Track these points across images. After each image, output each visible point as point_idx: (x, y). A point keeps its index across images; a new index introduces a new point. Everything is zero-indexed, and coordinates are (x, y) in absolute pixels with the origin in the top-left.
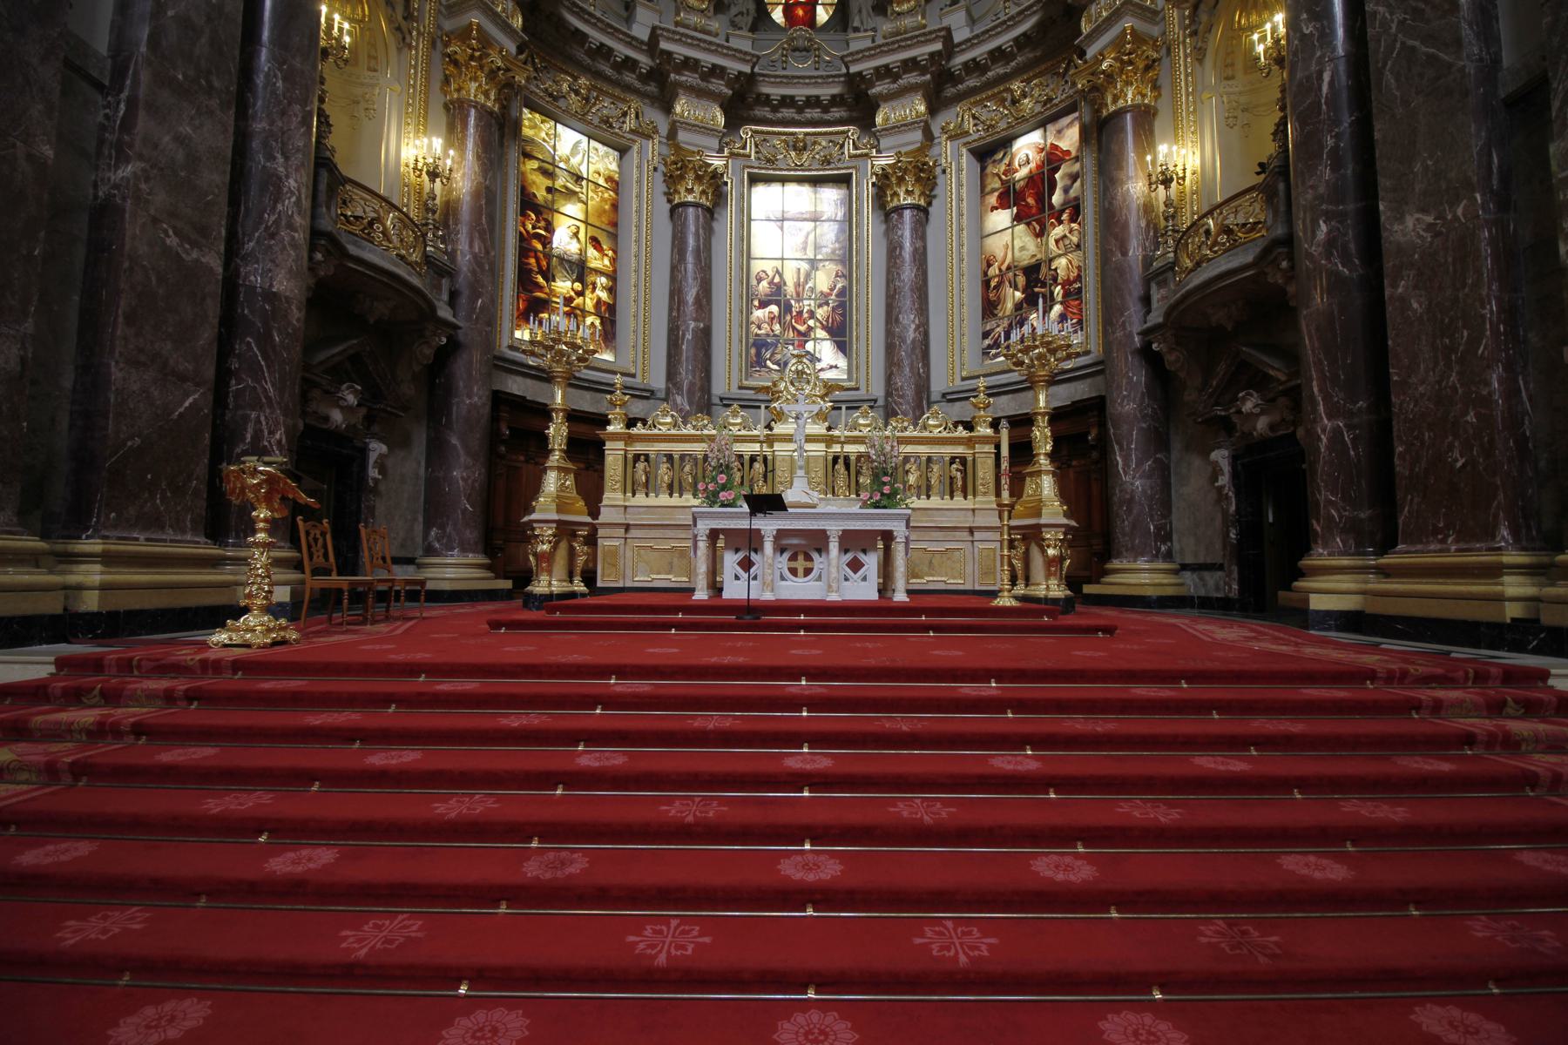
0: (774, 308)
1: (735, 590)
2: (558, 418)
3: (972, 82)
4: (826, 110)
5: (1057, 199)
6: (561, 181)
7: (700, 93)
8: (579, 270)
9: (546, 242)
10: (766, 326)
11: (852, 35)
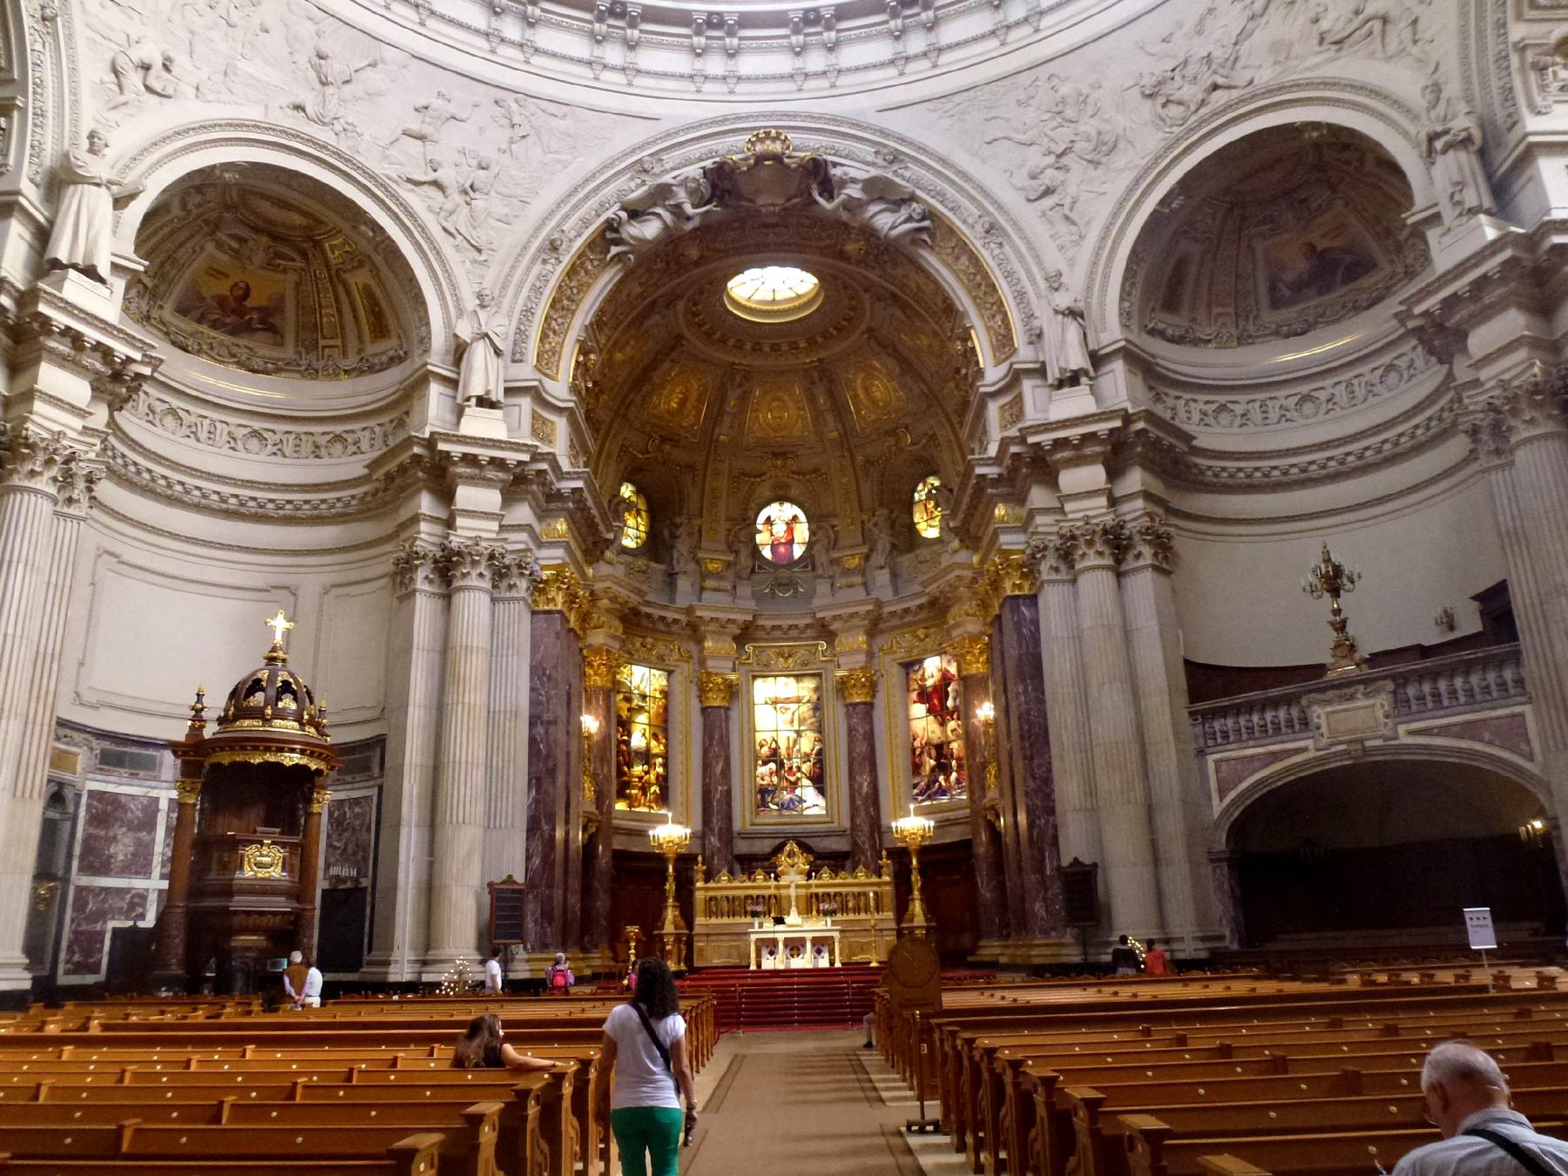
0: (772, 766)
1: (769, 963)
2: (671, 879)
3: (896, 622)
4: (803, 632)
5: (950, 703)
6: (636, 702)
7: (720, 634)
8: (646, 757)
9: (627, 743)
10: (767, 778)
11: (819, 581)
